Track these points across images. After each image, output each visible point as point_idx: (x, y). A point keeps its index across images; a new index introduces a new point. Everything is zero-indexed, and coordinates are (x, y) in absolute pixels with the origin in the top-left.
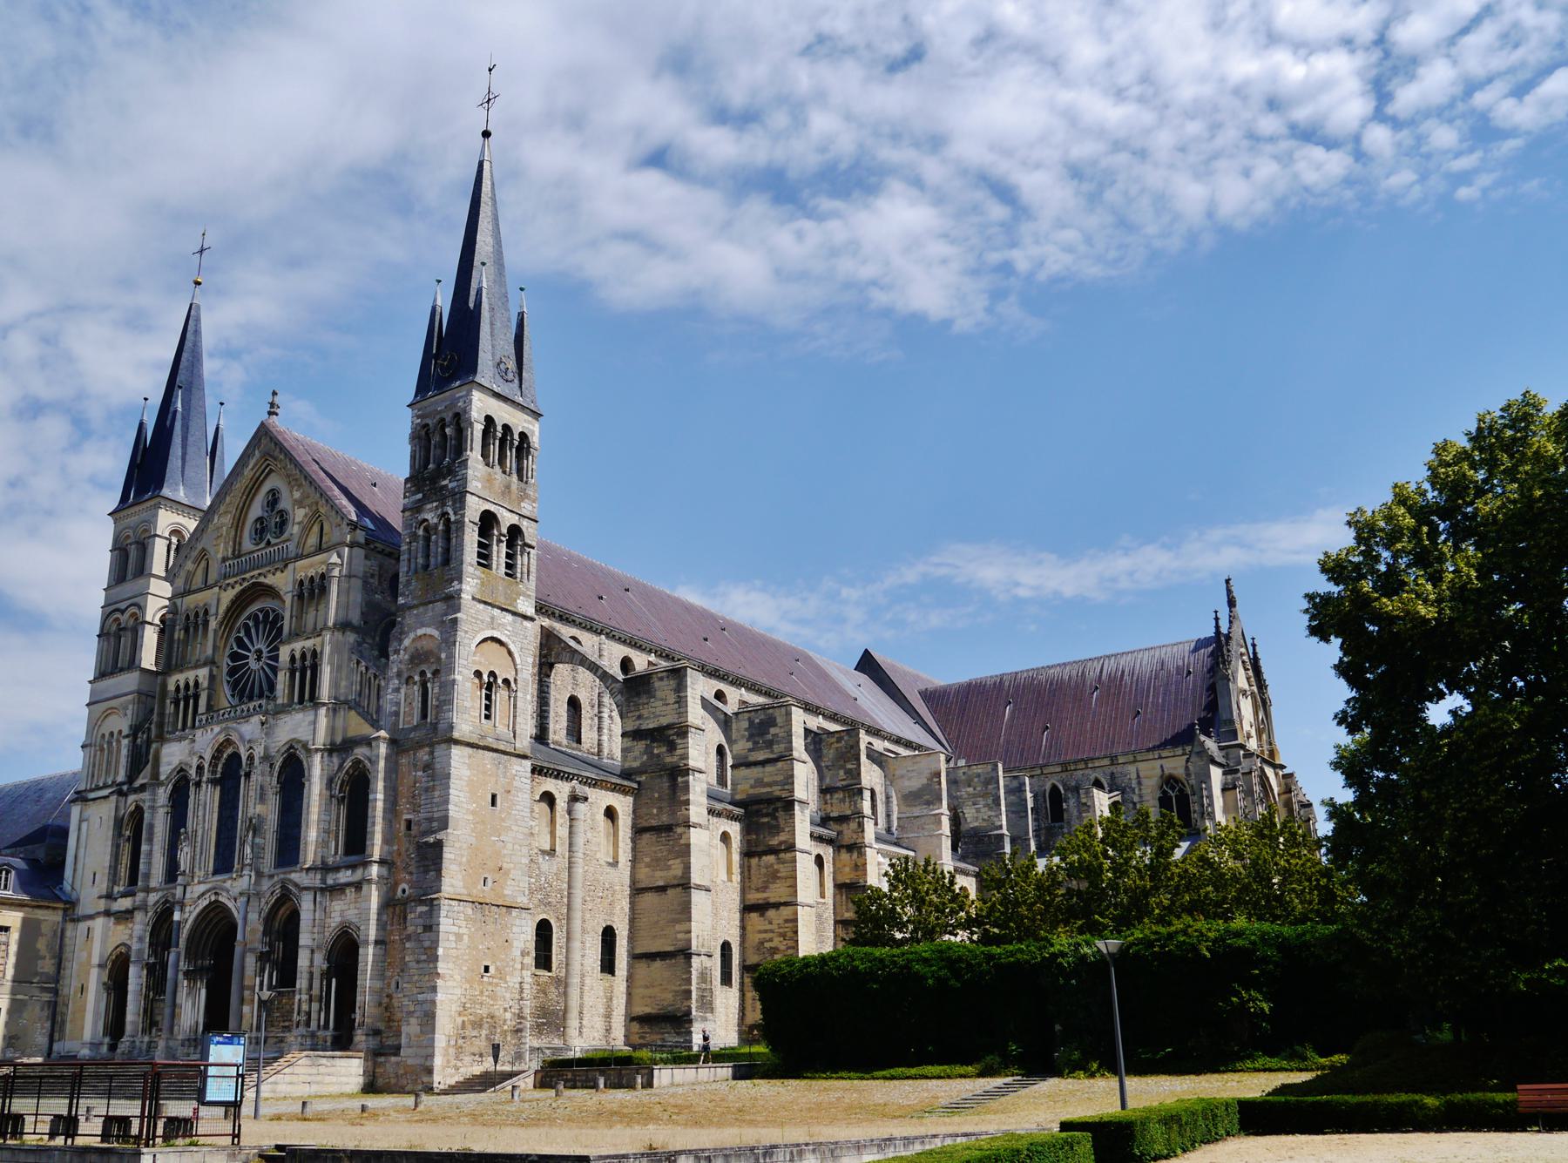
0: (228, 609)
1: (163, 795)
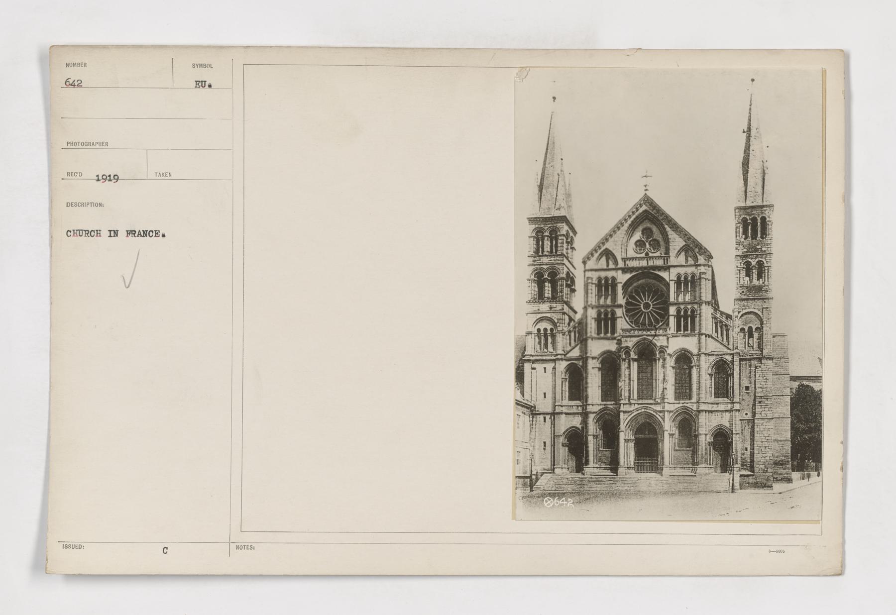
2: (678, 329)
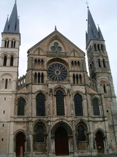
0: (49, 61)
1: (34, 96)
2: (74, 83)
